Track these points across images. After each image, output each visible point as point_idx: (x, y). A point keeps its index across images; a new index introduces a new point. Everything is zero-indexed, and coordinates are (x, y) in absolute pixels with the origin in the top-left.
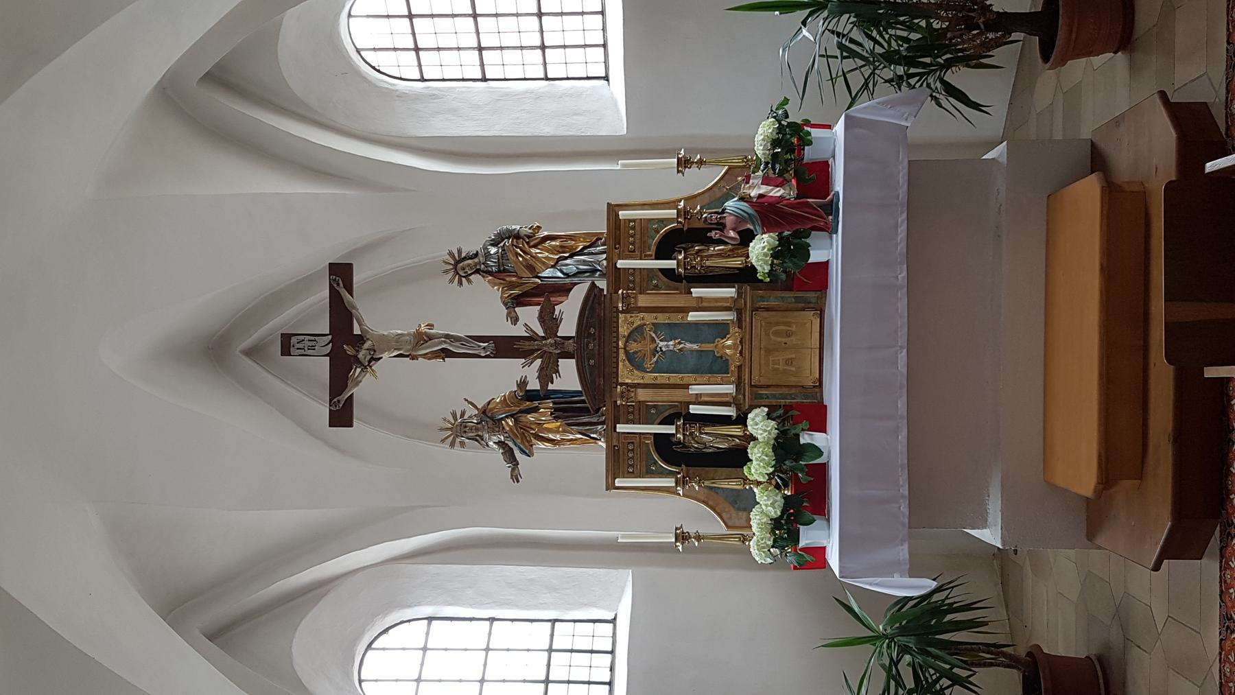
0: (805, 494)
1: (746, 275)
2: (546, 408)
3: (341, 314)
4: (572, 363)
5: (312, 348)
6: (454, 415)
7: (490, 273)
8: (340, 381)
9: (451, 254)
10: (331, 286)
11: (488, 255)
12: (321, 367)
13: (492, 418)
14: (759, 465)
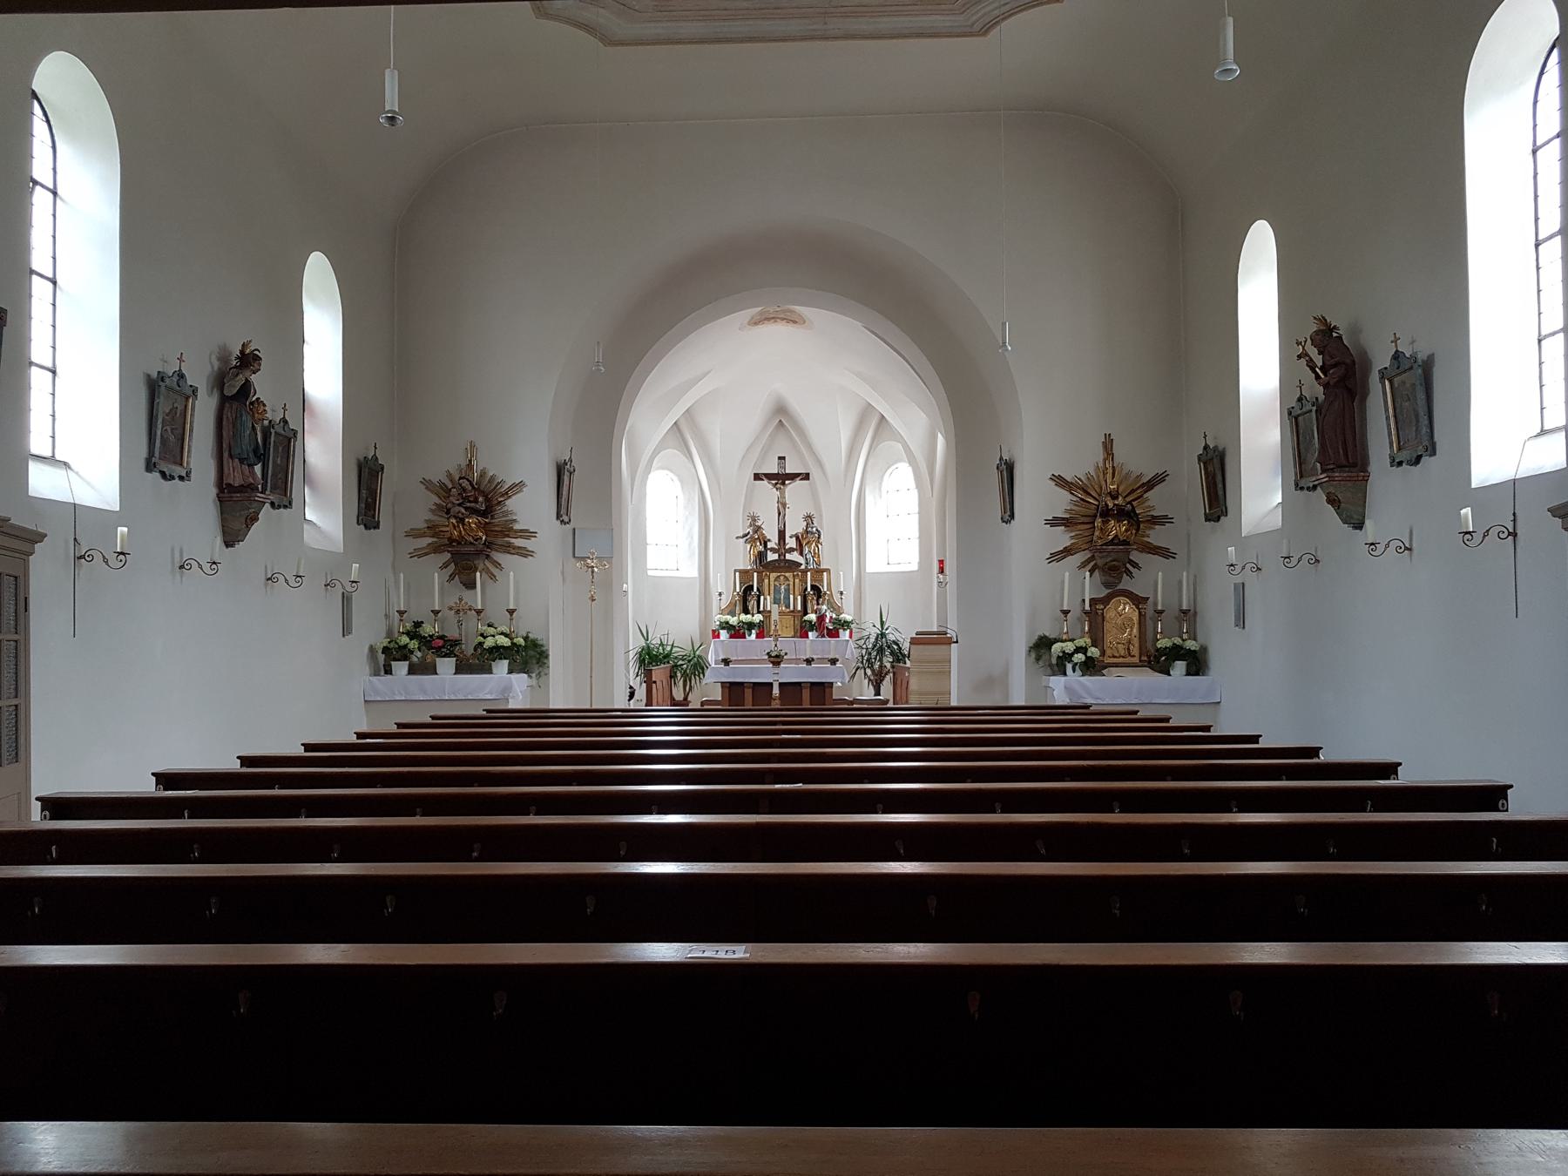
0: (737, 632)
1: (806, 613)
2: (761, 548)
3: (793, 477)
8: (769, 477)
14: (745, 618)
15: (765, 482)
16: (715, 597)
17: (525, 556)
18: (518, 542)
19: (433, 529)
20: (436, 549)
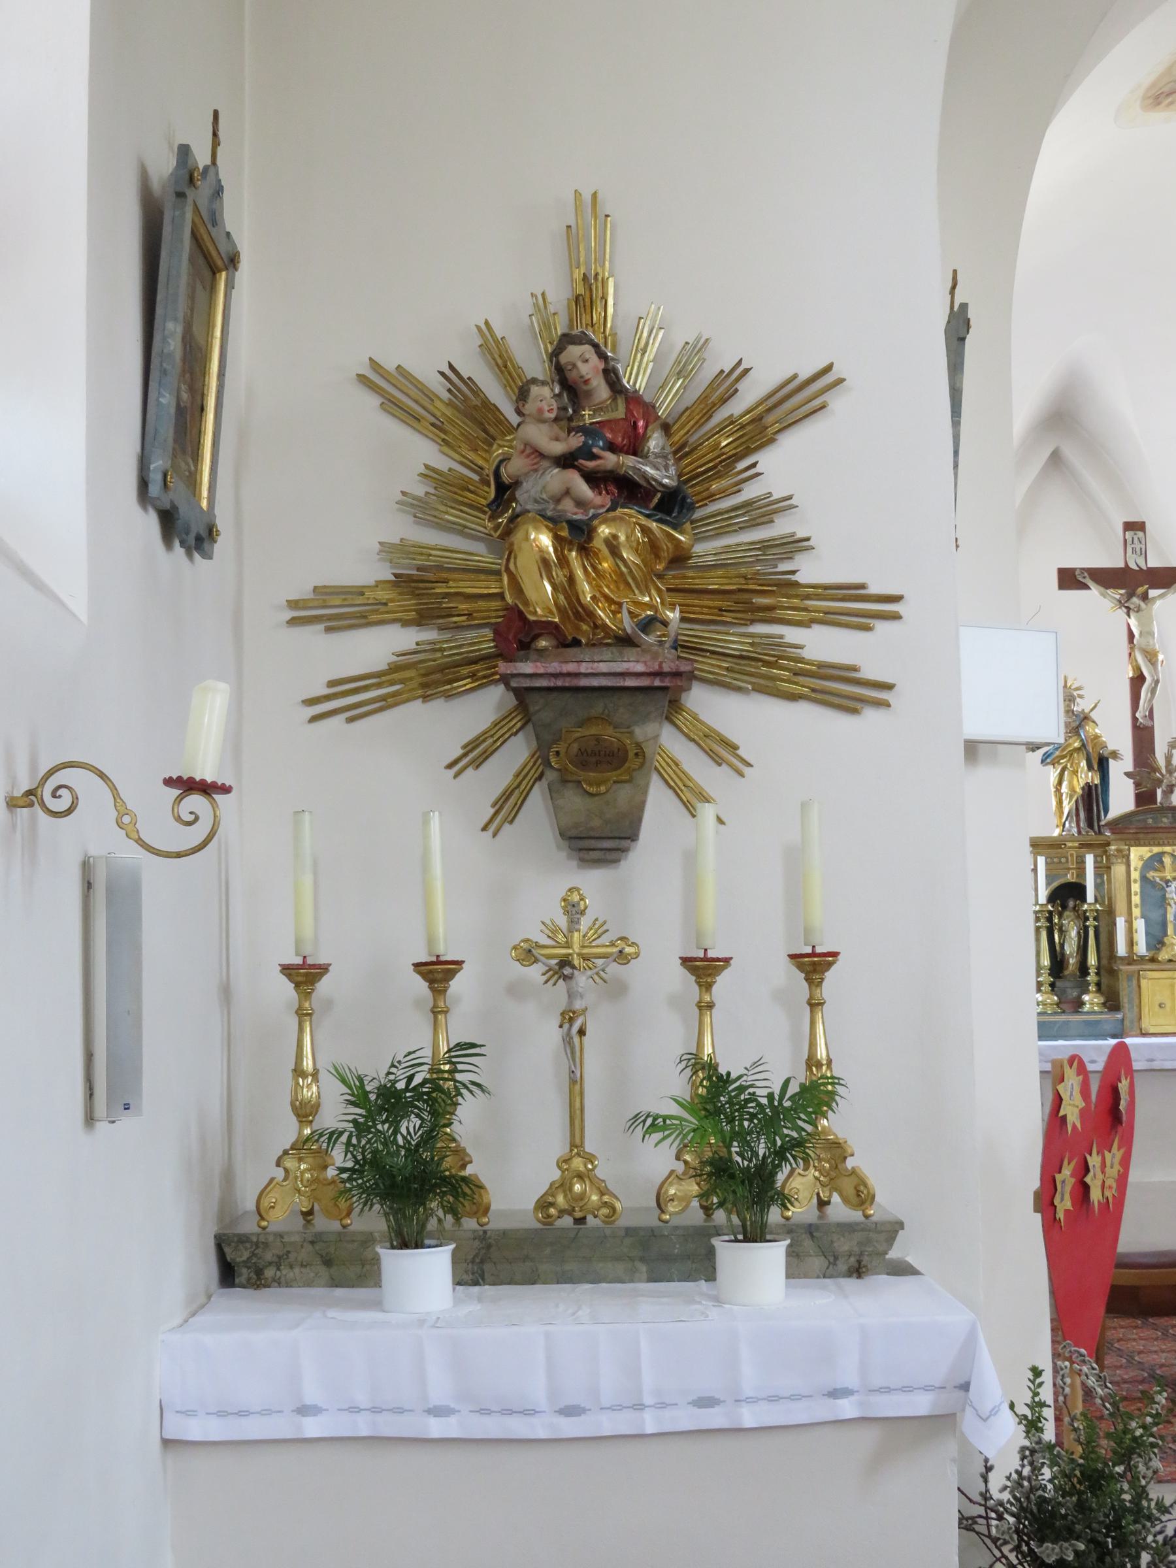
5: (1134, 551)
8: (1106, 578)
12: (1112, 559)
13: (1080, 726)
15: (1095, 591)
17: (850, 706)
18: (820, 644)
19: (418, 590)
20: (430, 678)
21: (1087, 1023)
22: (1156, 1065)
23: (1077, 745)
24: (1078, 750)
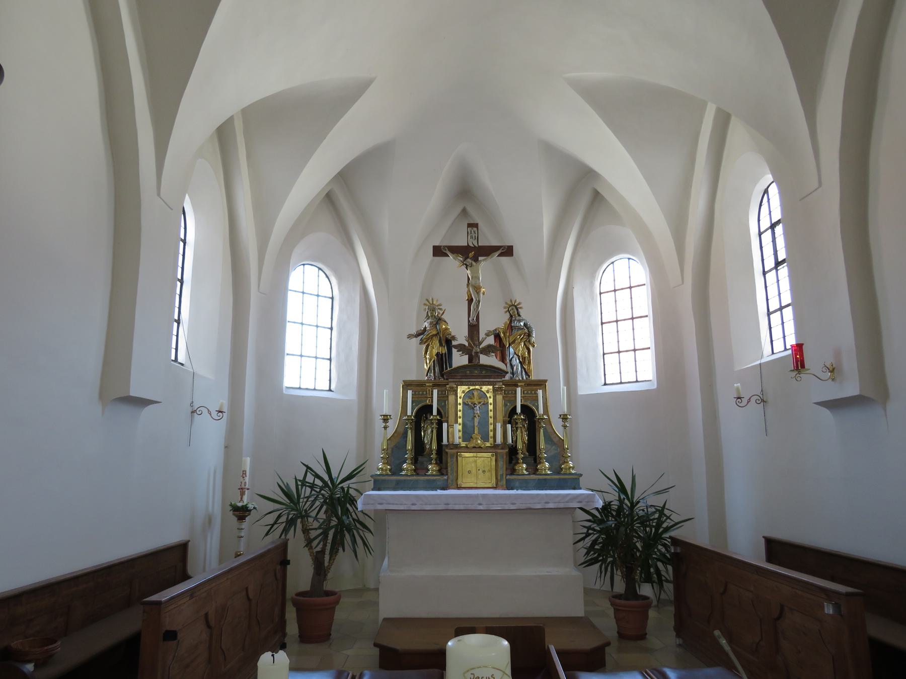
2: (444, 350)
4: (467, 363)
5: (472, 237)
6: (440, 305)
7: (511, 322)
9: (519, 304)
10: (500, 247)
11: (519, 321)
13: (437, 323)
16: (379, 424)
21: (428, 481)
22: (450, 507)
23: (434, 333)
24: (436, 335)
